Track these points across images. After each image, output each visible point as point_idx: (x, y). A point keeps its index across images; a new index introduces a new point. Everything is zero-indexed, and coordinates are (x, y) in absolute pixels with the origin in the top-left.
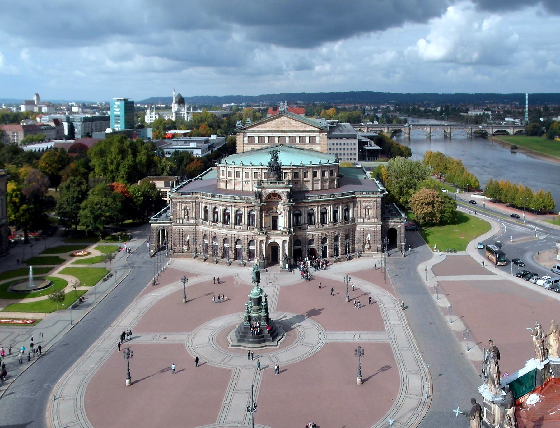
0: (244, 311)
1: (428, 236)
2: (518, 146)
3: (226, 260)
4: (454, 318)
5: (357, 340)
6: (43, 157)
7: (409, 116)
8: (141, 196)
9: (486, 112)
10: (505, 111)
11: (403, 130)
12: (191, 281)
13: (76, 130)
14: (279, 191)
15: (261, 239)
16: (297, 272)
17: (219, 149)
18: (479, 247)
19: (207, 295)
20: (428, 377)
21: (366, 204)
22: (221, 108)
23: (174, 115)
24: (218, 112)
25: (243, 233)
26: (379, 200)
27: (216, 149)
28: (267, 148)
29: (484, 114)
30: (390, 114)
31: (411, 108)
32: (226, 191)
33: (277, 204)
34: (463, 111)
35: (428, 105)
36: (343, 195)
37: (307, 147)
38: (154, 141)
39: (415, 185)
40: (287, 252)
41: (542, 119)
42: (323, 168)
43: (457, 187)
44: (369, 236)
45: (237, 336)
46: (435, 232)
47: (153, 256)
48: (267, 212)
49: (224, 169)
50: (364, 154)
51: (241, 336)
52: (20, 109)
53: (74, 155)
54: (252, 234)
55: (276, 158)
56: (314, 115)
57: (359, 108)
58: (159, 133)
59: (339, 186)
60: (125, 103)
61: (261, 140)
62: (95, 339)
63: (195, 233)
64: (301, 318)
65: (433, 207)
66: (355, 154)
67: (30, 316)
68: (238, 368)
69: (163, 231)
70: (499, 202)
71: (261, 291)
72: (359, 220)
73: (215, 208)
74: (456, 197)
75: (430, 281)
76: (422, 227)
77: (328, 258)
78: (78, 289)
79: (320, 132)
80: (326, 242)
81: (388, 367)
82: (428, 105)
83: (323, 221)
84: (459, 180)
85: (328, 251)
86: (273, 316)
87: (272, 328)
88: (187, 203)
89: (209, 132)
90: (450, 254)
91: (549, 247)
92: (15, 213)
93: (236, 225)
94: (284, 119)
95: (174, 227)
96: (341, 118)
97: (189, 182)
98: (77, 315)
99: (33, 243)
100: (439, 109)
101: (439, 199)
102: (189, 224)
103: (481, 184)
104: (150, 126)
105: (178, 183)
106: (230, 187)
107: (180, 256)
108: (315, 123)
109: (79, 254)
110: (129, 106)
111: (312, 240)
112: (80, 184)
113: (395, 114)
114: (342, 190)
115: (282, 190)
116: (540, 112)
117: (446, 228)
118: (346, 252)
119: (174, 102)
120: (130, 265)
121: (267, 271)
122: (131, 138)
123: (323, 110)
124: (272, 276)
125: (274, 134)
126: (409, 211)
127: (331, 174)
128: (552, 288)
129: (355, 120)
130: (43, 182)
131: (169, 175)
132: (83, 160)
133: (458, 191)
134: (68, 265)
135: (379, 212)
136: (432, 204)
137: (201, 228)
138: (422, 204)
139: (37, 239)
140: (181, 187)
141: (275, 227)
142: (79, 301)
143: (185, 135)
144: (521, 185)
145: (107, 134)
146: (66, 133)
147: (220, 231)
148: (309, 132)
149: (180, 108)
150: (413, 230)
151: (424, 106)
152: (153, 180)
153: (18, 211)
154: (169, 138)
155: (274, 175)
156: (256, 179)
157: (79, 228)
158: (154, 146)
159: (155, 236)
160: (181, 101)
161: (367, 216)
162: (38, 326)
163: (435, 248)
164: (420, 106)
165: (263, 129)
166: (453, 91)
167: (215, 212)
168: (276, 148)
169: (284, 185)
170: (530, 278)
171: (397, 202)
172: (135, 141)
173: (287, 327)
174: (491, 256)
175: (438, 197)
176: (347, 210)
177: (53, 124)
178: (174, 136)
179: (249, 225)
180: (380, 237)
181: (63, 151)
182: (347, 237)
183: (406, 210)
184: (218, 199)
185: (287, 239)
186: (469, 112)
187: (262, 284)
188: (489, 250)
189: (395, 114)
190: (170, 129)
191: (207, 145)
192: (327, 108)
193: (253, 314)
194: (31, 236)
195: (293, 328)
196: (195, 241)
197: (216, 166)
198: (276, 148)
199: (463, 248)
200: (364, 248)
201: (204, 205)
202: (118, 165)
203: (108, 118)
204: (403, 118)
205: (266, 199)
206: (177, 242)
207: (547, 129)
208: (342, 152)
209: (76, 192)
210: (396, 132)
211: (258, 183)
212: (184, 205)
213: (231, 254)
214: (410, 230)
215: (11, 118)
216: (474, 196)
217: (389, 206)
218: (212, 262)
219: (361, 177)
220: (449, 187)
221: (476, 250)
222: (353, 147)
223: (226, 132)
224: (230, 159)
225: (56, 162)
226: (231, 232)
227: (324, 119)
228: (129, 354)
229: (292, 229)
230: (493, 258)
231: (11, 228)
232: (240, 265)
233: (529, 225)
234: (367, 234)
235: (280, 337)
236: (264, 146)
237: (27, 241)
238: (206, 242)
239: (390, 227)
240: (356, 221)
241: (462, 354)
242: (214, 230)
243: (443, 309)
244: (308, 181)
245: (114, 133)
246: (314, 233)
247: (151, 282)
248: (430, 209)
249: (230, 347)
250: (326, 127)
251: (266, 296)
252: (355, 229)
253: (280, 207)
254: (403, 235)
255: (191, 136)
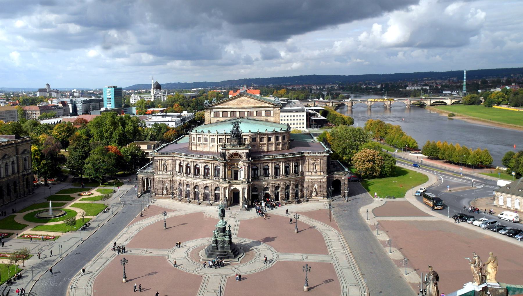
0: (211, 236)
1: (370, 185)
2: (455, 113)
3: (196, 201)
4: (393, 249)
5: (305, 260)
6: (56, 128)
7: (352, 93)
8: (129, 155)
9: (424, 87)
10: (442, 86)
11: (346, 104)
12: (170, 215)
13: (78, 109)
14: (240, 152)
15: (225, 186)
16: (254, 210)
17: (189, 122)
18: (417, 194)
19: (182, 224)
20: (366, 289)
21: (314, 161)
22: (190, 92)
23: (153, 97)
24: (188, 94)
25: (210, 182)
26: (325, 158)
27: (187, 121)
28: (230, 120)
29: (422, 89)
30: (334, 92)
31: (353, 86)
32: (197, 152)
33: (238, 161)
34: (402, 87)
35: (369, 84)
36: (293, 154)
37: (263, 119)
38: (138, 116)
39: (357, 146)
40: (246, 196)
41: (480, 91)
42: (277, 135)
43: (396, 147)
44: (316, 185)
45: (206, 253)
46: (376, 183)
47: (140, 197)
48: (230, 167)
49: (195, 136)
50: (310, 123)
51: (209, 254)
52: (36, 95)
53: (78, 127)
54: (217, 183)
55: (237, 127)
56: (267, 94)
57: (307, 88)
58: (141, 110)
59: (290, 147)
60: (115, 90)
61: (225, 114)
62: (100, 251)
63: (173, 182)
64: (258, 243)
65: (374, 163)
66: (303, 124)
67: (51, 234)
68: (208, 275)
69: (147, 179)
70: (437, 159)
71: (226, 223)
72: (307, 173)
73: (188, 164)
74: (395, 155)
75: (371, 221)
76: (363, 179)
77: (280, 201)
78: (85, 217)
79: (274, 108)
80: (278, 189)
81: (331, 280)
82: (369, 84)
83: (276, 174)
84: (399, 143)
85: (280, 196)
86: (235, 241)
87: (234, 249)
88: (165, 160)
89: (181, 109)
90: (389, 200)
91: (486, 195)
92: (38, 166)
93: (204, 176)
94: (244, 98)
95: (156, 177)
96: (291, 96)
97: (167, 145)
98: (85, 235)
99: (51, 186)
100: (379, 86)
101: (380, 157)
102: (168, 175)
103: (419, 145)
104: (134, 105)
105: (158, 145)
106: (200, 149)
107: (161, 198)
108: (270, 100)
109: (85, 194)
110: (118, 91)
111: (267, 188)
112: (83, 147)
113: (338, 92)
114: (293, 151)
115: (242, 151)
116: (479, 84)
117: (386, 179)
118: (296, 196)
119: (152, 88)
120: (123, 203)
121: (229, 209)
122: (120, 114)
123: (275, 91)
124: (234, 213)
125: (235, 110)
126: (353, 167)
127: (284, 138)
128: (488, 228)
129: (304, 99)
130: (57, 145)
131: (151, 140)
132: (84, 130)
133: (397, 151)
134: (77, 201)
135: (325, 167)
136: (373, 161)
137: (177, 178)
138: (364, 161)
139: (53, 184)
140: (161, 149)
141: (236, 178)
142: (85, 227)
143: (162, 111)
144: (458, 146)
145: (101, 112)
146: (71, 111)
147: (192, 180)
148: (265, 107)
149: (158, 92)
150: (355, 181)
151: (366, 84)
152: (138, 144)
153: (40, 165)
154: (149, 114)
155: (235, 140)
156: (221, 143)
157: (84, 177)
158: (138, 120)
159: (141, 183)
160: (158, 87)
161: (315, 171)
162: (57, 240)
163: (376, 195)
164: (361, 85)
165: (226, 106)
166: (393, 72)
167: (187, 167)
168: (237, 120)
169: (244, 147)
170: (466, 220)
171: (341, 159)
172: (123, 116)
173: (246, 249)
174: (428, 201)
175: (378, 156)
176: (297, 166)
177: (61, 105)
178: (153, 112)
179: (215, 176)
180: (325, 186)
181: (69, 124)
182: (297, 186)
183: (349, 166)
184: (190, 158)
185: (246, 187)
186: (408, 88)
187: (225, 219)
188: (426, 197)
189: (338, 92)
190: (150, 108)
191: (179, 119)
192: (278, 89)
193: (219, 239)
194: (49, 181)
195: (251, 250)
196: (172, 187)
197: (187, 134)
198: (237, 120)
199: (403, 195)
200: (311, 194)
201: (179, 162)
202: (111, 133)
203: (102, 100)
204: (346, 94)
205: (229, 158)
206: (158, 187)
207: (485, 98)
208: (292, 122)
209: (81, 152)
210: (341, 106)
211: (222, 146)
212: (163, 162)
213: (201, 197)
214: (352, 181)
215: (30, 101)
216: (412, 155)
217: (333, 163)
218: (186, 202)
219: (309, 141)
220: (389, 147)
221: (414, 197)
222: (301, 118)
223: (194, 109)
224: (199, 129)
225: (65, 132)
226: (201, 181)
227: (277, 98)
228: (124, 262)
229: (250, 180)
230: (431, 203)
231: (35, 176)
232: (208, 204)
233: (466, 177)
234: (314, 184)
235: (240, 256)
236: (227, 119)
237: (46, 184)
238: (181, 187)
239: (335, 179)
240: (305, 174)
241: (400, 277)
242: (187, 180)
243: (383, 242)
244: (263, 144)
245: (107, 110)
246: (268, 182)
247: (139, 214)
248: (371, 165)
249: (201, 260)
250: (280, 104)
251: (229, 226)
252: (304, 180)
253: (240, 164)
254: (346, 185)
255: (166, 112)
